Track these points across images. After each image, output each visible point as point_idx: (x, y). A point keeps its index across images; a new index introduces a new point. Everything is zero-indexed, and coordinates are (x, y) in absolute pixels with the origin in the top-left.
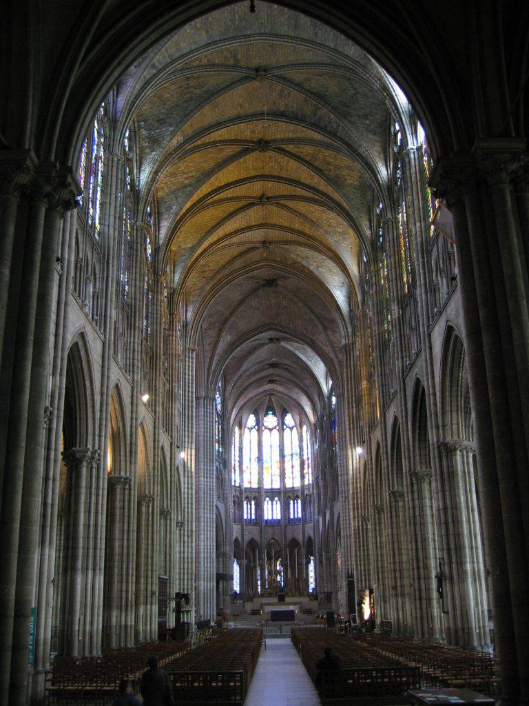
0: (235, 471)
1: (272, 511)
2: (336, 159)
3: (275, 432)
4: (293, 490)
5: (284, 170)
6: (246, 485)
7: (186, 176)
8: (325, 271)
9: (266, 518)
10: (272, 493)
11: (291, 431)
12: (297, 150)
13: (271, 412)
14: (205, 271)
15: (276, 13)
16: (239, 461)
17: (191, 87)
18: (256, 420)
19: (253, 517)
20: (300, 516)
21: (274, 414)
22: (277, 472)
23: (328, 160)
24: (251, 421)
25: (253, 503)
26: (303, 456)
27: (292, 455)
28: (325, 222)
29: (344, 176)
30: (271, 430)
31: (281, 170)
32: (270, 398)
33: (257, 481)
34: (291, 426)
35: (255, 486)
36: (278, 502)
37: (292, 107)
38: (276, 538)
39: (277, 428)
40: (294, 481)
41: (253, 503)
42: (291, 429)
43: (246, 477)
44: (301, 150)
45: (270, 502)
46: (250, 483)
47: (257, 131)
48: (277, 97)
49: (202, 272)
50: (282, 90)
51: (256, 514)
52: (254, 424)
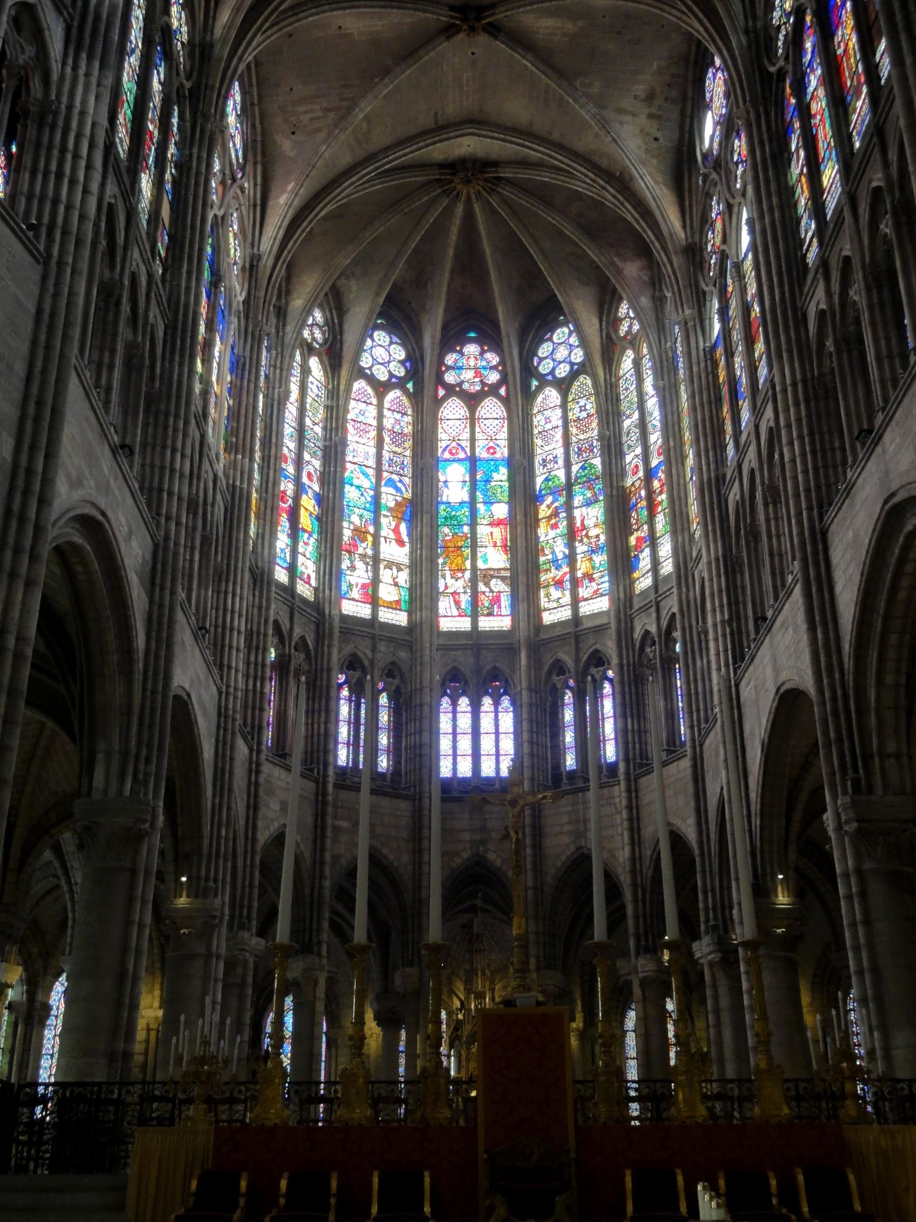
1: (477, 741)
3: (492, 409)
4: (577, 630)
6: (354, 607)
9: (445, 771)
10: (479, 667)
11: (564, 394)
13: (472, 335)
16: (320, 499)
18: (409, 358)
19: (383, 763)
20: (610, 752)
21: (490, 338)
22: (495, 558)
25: (383, 699)
26: (623, 474)
27: (569, 486)
30: (472, 400)
32: (469, 217)
33: (405, 595)
34: (563, 371)
35: (401, 619)
36: (506, 702)
38: (491, 856)
39: (502, 391)
40: (577, 595)
41: (383, 699)
42: (564, 386)
43: (357, 575)
45: (464, 703)
46: (374, 600)
51: (395, 750)
52: (401, 372)
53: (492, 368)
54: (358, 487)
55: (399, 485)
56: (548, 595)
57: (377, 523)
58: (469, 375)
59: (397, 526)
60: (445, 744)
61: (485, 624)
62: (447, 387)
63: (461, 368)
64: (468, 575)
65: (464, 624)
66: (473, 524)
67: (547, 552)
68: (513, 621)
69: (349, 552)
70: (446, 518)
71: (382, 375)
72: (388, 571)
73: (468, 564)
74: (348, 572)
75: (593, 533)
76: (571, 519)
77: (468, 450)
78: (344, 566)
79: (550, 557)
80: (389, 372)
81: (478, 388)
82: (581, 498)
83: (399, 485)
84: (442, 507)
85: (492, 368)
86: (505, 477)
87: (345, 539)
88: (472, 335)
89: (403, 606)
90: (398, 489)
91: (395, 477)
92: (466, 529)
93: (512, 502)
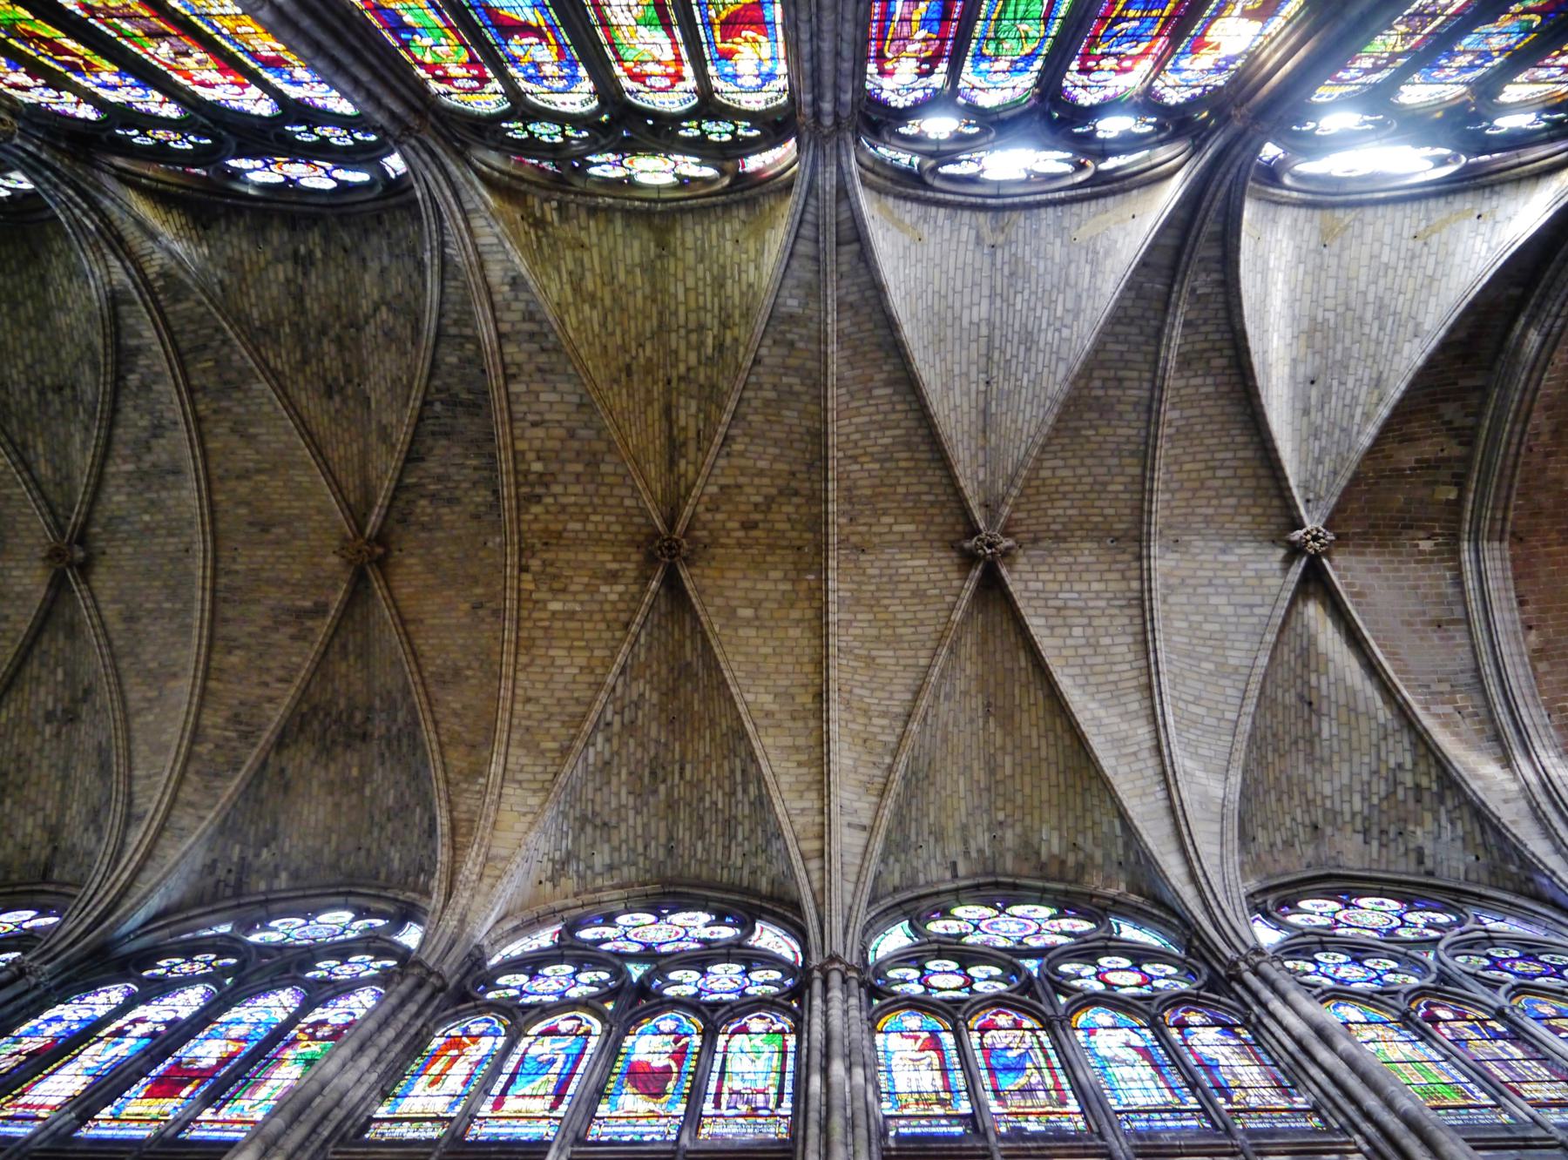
2: (701, 328)
5: (794, 484)
7: (739, 788)
8: (1433, 300)
12: (692, 446)
14: (1418, 787)
15: (160, 517)
17: (388, 730)
23: (709, 351)
28: (1066, 332)
29: (742, 294)
31: (796, 493)
37: (475, 469)
44: (692, 433)
47: (615, 566)
48: (457, 509)
49: (1418, 801)
50: (433, 497)
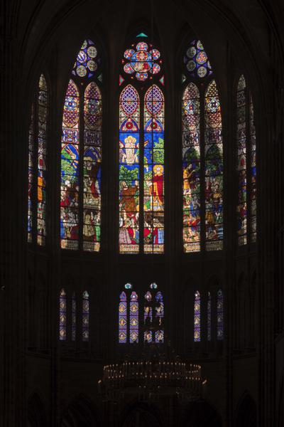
0: (35, 202)
3: (156, 95)
13: (143, 35)
22: (156, 205)
24: (86, 56)
30: (142, 87)
36: (159, 296)
39: (162, 80)
43: (67, 221)
45: (134, 296)
53: (157, 62)
54: (68, 160)
55: (94, 153)
56: (187, 233)
57: (82, 187)
58: (140, 67)
59: (94, 184)
60: (122, 323)
61: (148, 249)
62: (126, 76)
63: (135, 61)
64: (137, 215)
65: (135, 249)
66: (141, 180)
67: (187, 203)
68: (165, 248)
69: (65, 207)
70: (123, 175)
71: (81, 72)
72: (87, 217)
73: (138, 207)
74: (64, 221)
75: (216, 196)
76: (203, 183)
77: (138, 124)
78: (62, 217)
79: (189, 207)
80: (87, 69)
81: (145, 77)
82: (210, 170)
83: (94, 153)
84: (122, 167)
85: (157, 62)
86: (162, 146)
87: (62, 198)
88: (143, 35)
89: (98, 239)
90: (93, 157)
91: (91, 148)
92: (137, 183)
93: (166, 165)
